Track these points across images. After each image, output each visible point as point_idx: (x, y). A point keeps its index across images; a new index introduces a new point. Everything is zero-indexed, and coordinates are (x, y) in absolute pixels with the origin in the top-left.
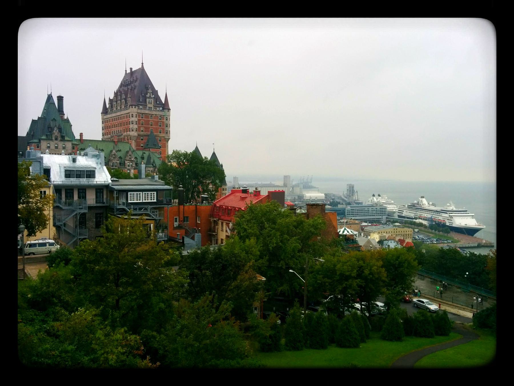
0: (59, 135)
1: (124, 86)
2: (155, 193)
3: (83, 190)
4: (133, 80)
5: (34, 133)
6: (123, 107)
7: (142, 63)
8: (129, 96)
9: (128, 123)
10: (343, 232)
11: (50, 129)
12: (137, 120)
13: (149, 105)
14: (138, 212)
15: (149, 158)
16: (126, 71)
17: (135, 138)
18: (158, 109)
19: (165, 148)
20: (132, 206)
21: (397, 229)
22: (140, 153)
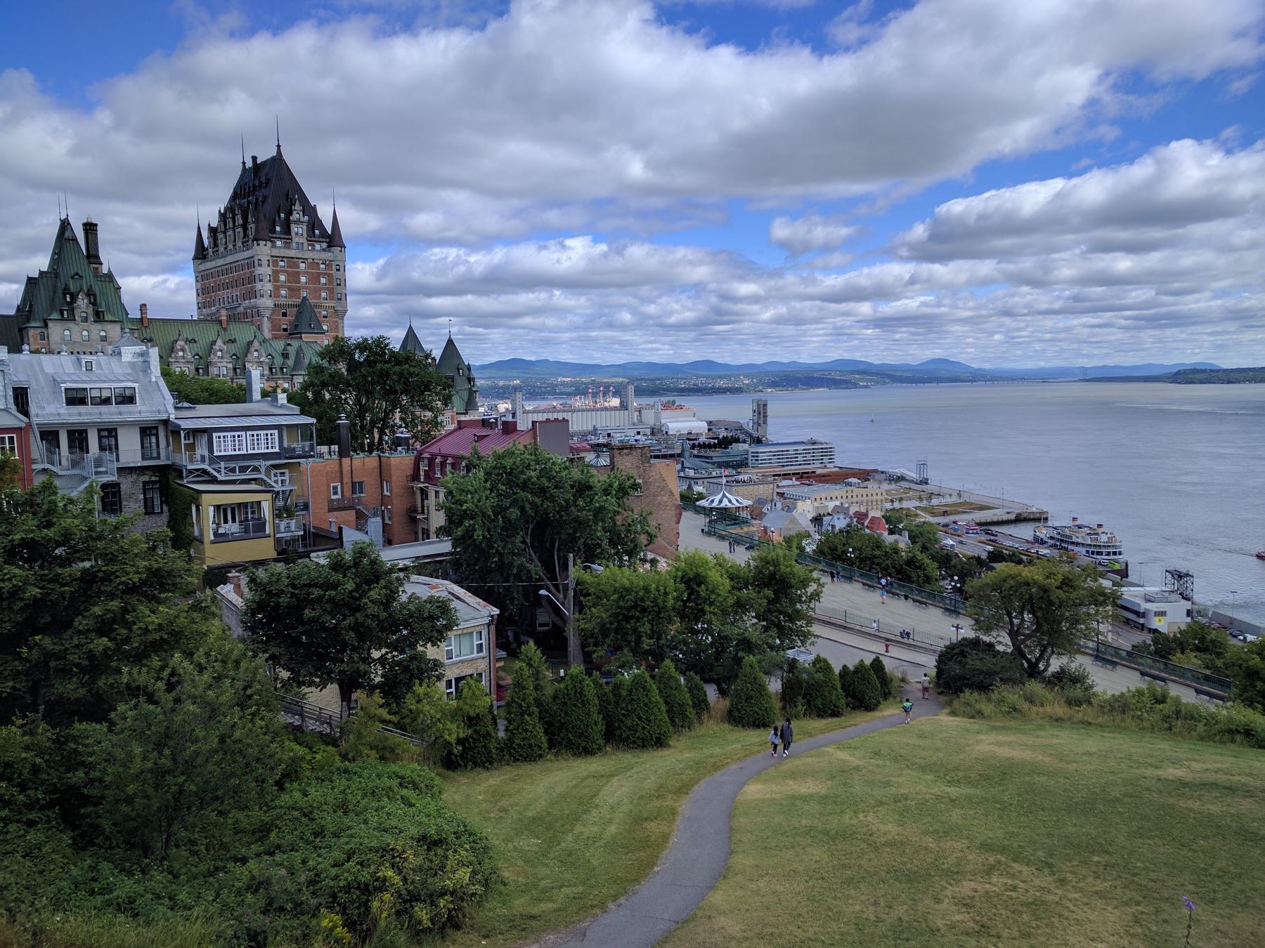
0: (90, 310)
2: (276, 432)
3: (109, 434)
5: (31, 306)
6: (239, 244)
7: (279, 146)
8: (250, 220)
10: (721, 501)
13: (296, 239)
16: (244, 163)
17: (268, 313)
18: (318, 247)
20: (222, 463)
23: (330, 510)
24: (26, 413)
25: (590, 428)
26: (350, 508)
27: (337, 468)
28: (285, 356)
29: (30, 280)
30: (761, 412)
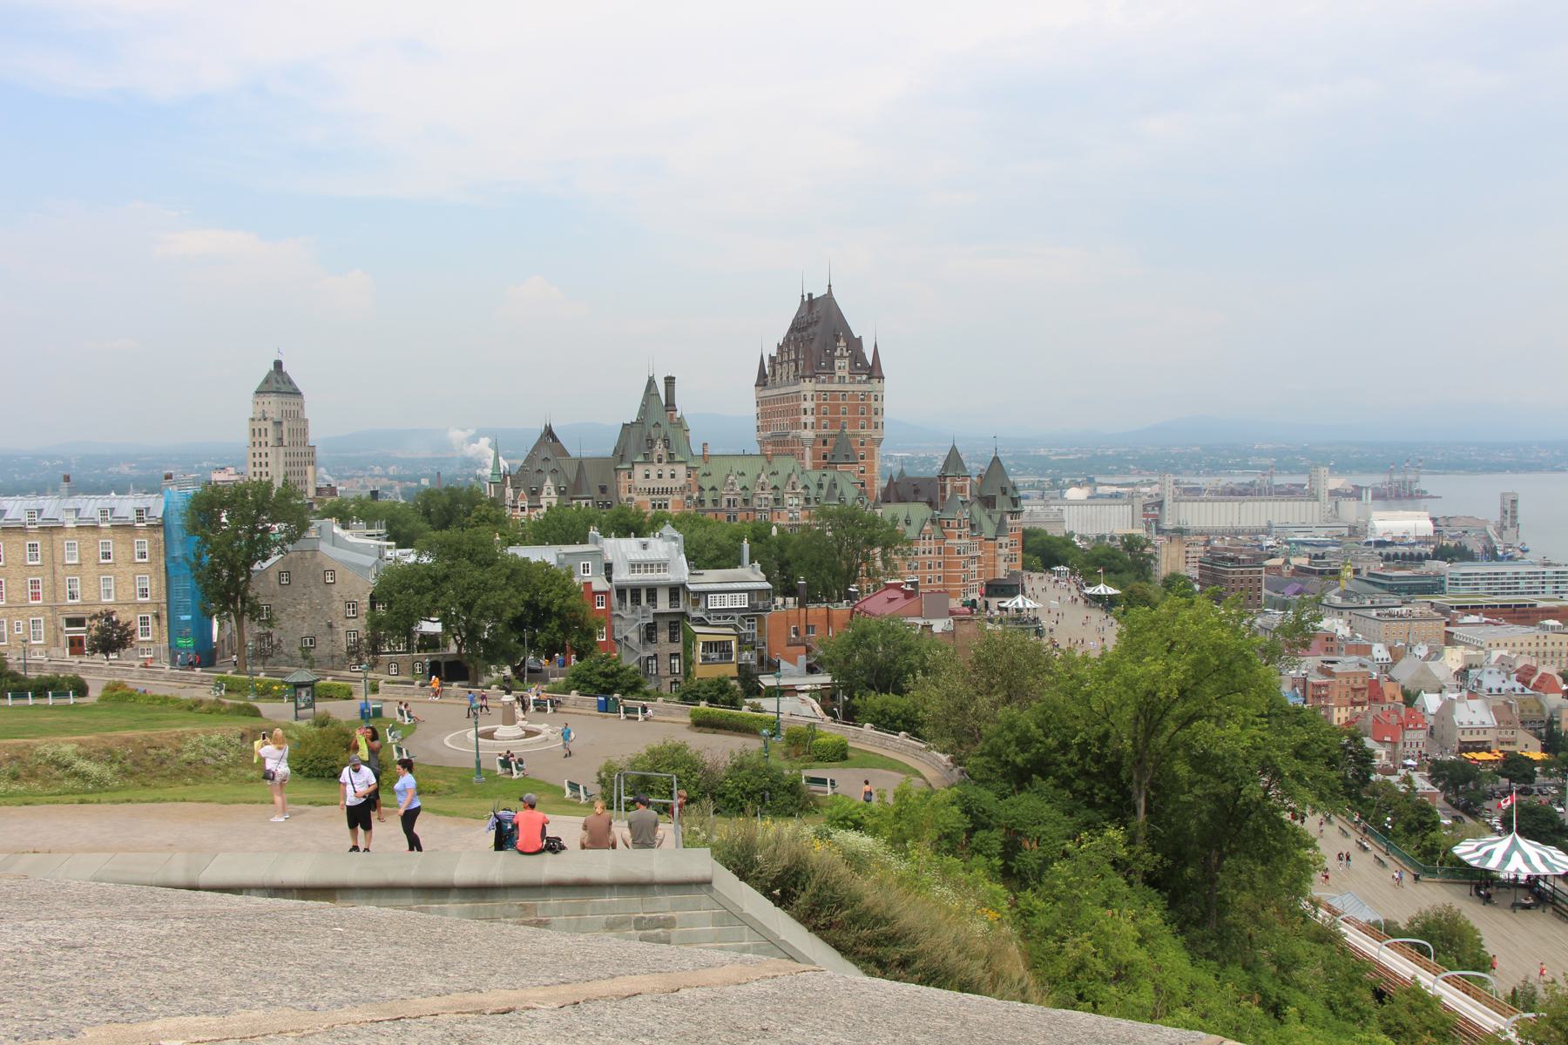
1: (799, 330)
3: (652, 592)
4: (812, 318)
6: (791, 377)
7: (830, 286)
11: (651, 443)
12: (813, 406)
13: (839, 373)
14: (722, 622)
16: (803, 296)
18: (858, 378)
21: (1546, 637)
22: (815, 476)
23: (788, 645)
24: (609, 580)
25: (1264, 524)
27: (796, 615)
28: (820, 486)
29: (624, 425)
30: (1510, 510)
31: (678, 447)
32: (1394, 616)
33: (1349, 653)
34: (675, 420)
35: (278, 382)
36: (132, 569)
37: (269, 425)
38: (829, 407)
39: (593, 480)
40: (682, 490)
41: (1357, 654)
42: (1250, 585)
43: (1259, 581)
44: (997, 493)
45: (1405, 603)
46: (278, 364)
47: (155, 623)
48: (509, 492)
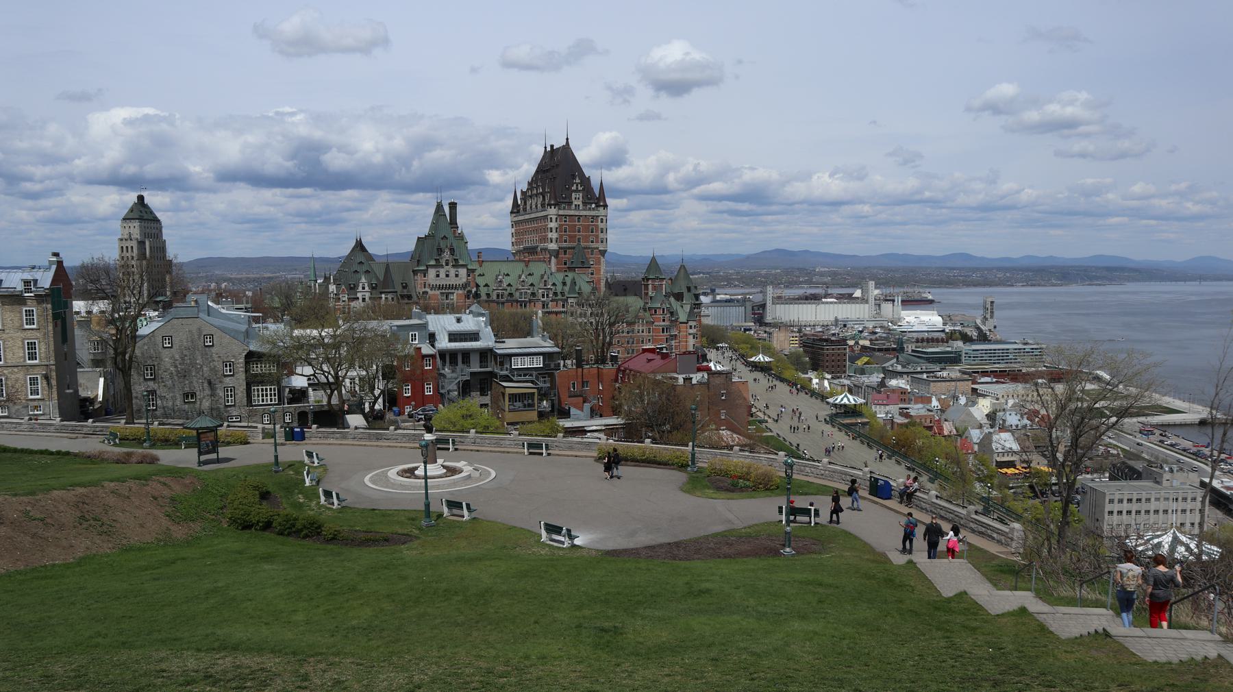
1: (544, 172)
3: (466, 354)
6: (539, 205)
7: (567, 139)
9: (545, 229)
11: (440, 251)
12: (557, 226)
13: (575, 202)
15: (574, 283)
16: (546, 148)
19: (600, 265)
22: (560, 277)
23: (570, 397)
25: (832, 319)
26: (580, 396)
27: (574, 373)
28: (564, 284)
29: (419, 238)
31: (460, 255)
32: (938, 378)
33: (916, 403)
34: (457, 235)
35: (141, 211)
36: (19, 334)
37: (134, 244)
38: (568, 228)
39: (397, 280)
40: (464, 286)
41: (922, 403)
42: (839, 358)
43: (845, 355)
44: (684, 290)
45: (942, 369)
46: (141, 198)
47: (45, 382)
48: (332, 288)
